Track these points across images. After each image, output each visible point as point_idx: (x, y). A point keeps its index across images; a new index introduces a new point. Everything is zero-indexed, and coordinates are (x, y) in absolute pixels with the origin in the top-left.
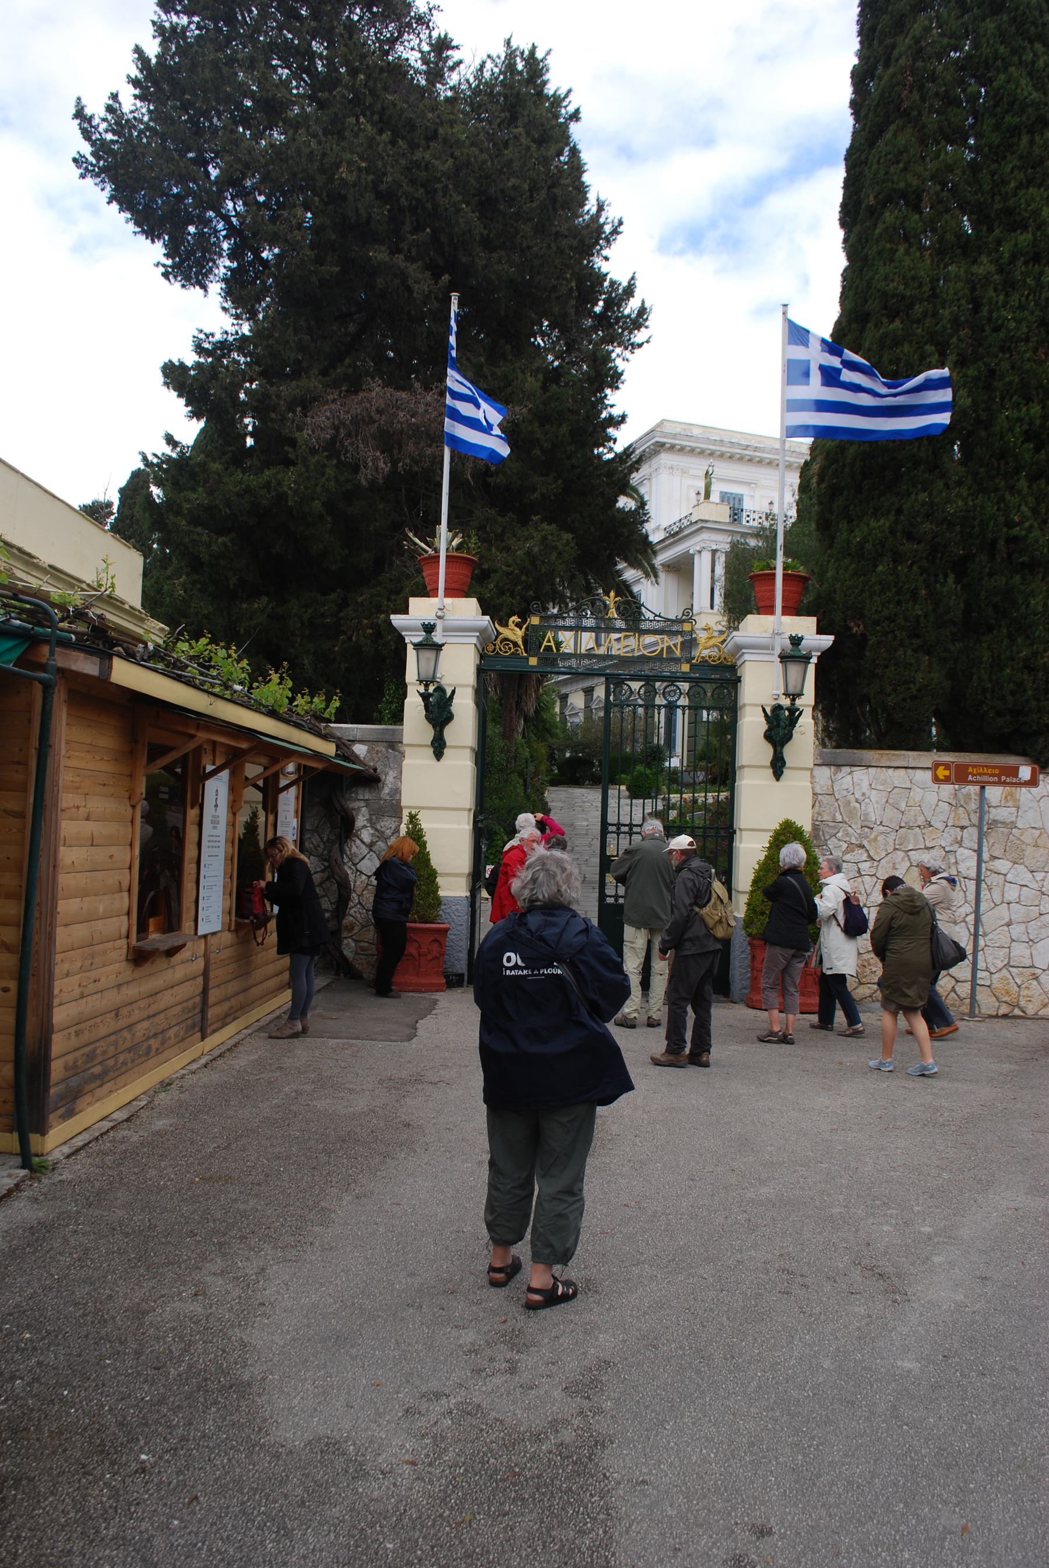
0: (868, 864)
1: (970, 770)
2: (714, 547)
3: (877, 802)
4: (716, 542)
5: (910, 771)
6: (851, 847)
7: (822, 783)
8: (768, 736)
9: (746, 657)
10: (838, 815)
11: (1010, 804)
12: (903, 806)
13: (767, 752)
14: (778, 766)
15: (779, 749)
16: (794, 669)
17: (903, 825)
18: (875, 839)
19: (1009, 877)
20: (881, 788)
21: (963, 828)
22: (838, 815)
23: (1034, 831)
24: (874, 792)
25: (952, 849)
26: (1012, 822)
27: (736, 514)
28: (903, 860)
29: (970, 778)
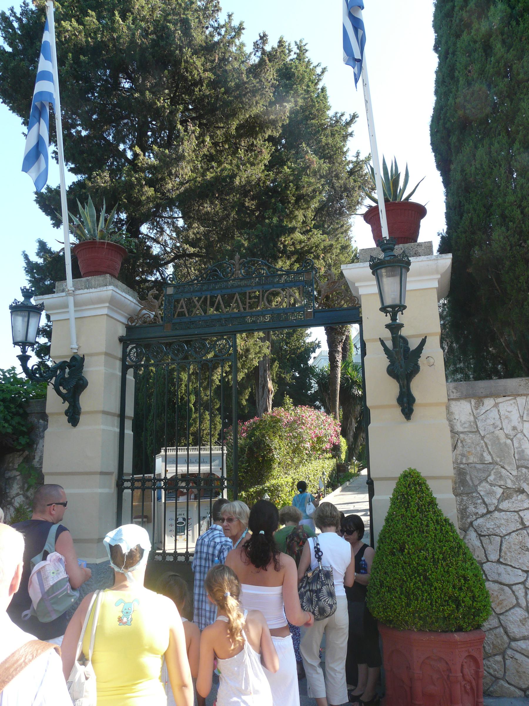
6: (506, 495)
7: (463, 419)
8: (391, 372)
10: (485, 454)
14: (406, 404)
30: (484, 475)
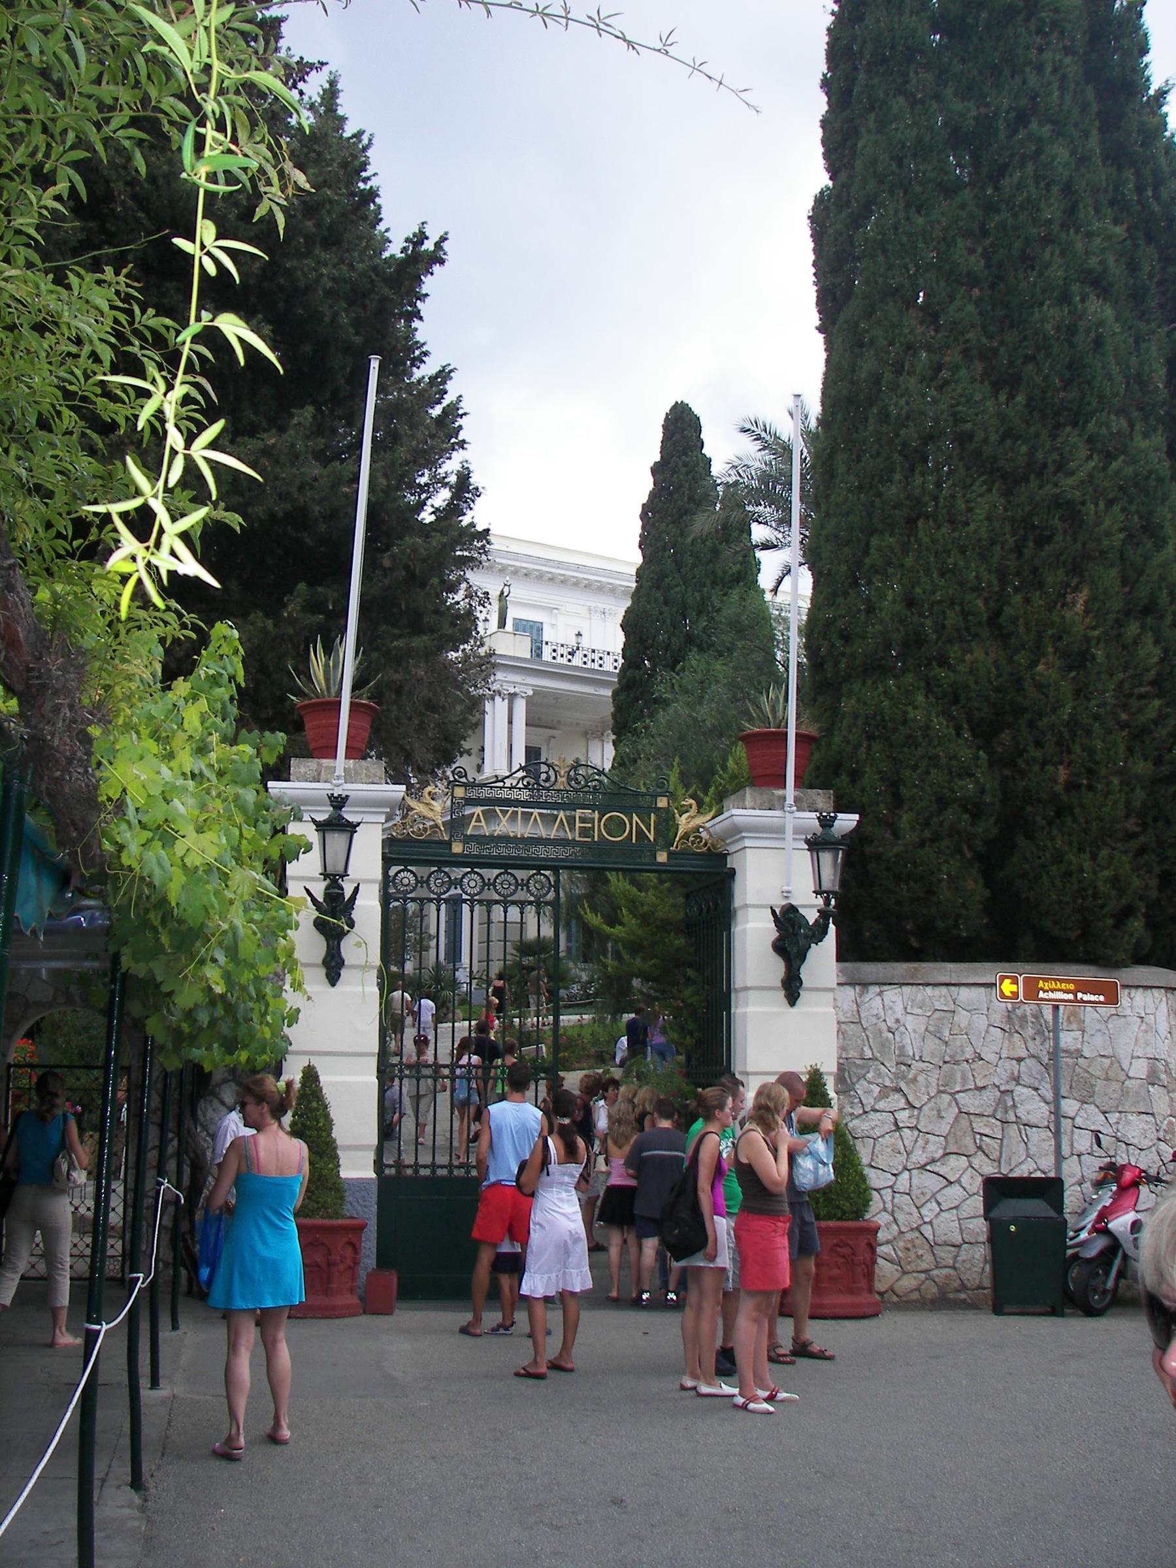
0: (907, 1113)
1: (1041, 984)
2: (512, 690)
3: (915, 1031)
4: (515, 684)
5: (953, 988)
6: (885, 1092)
8: (779, 947)
9: (747, 843)
10: (866, 1049)
11: (1074, 1026)
13: (777, 968)
14: (792, 988)
16: (826, 858)
17: (947, 1059)
18: (914, 1080)
19: (1079, 1121)
20: (919, 1011)
21: (1019, 1060)
22: (866, 1049)
23: (1103, 1060)
24: (909, 1017)
25: (1008, 1087)
26: (1078, 1050)
27: (537, 651)
28: (950, 1105)
29: (1041, 995)
30: (863, 1072)
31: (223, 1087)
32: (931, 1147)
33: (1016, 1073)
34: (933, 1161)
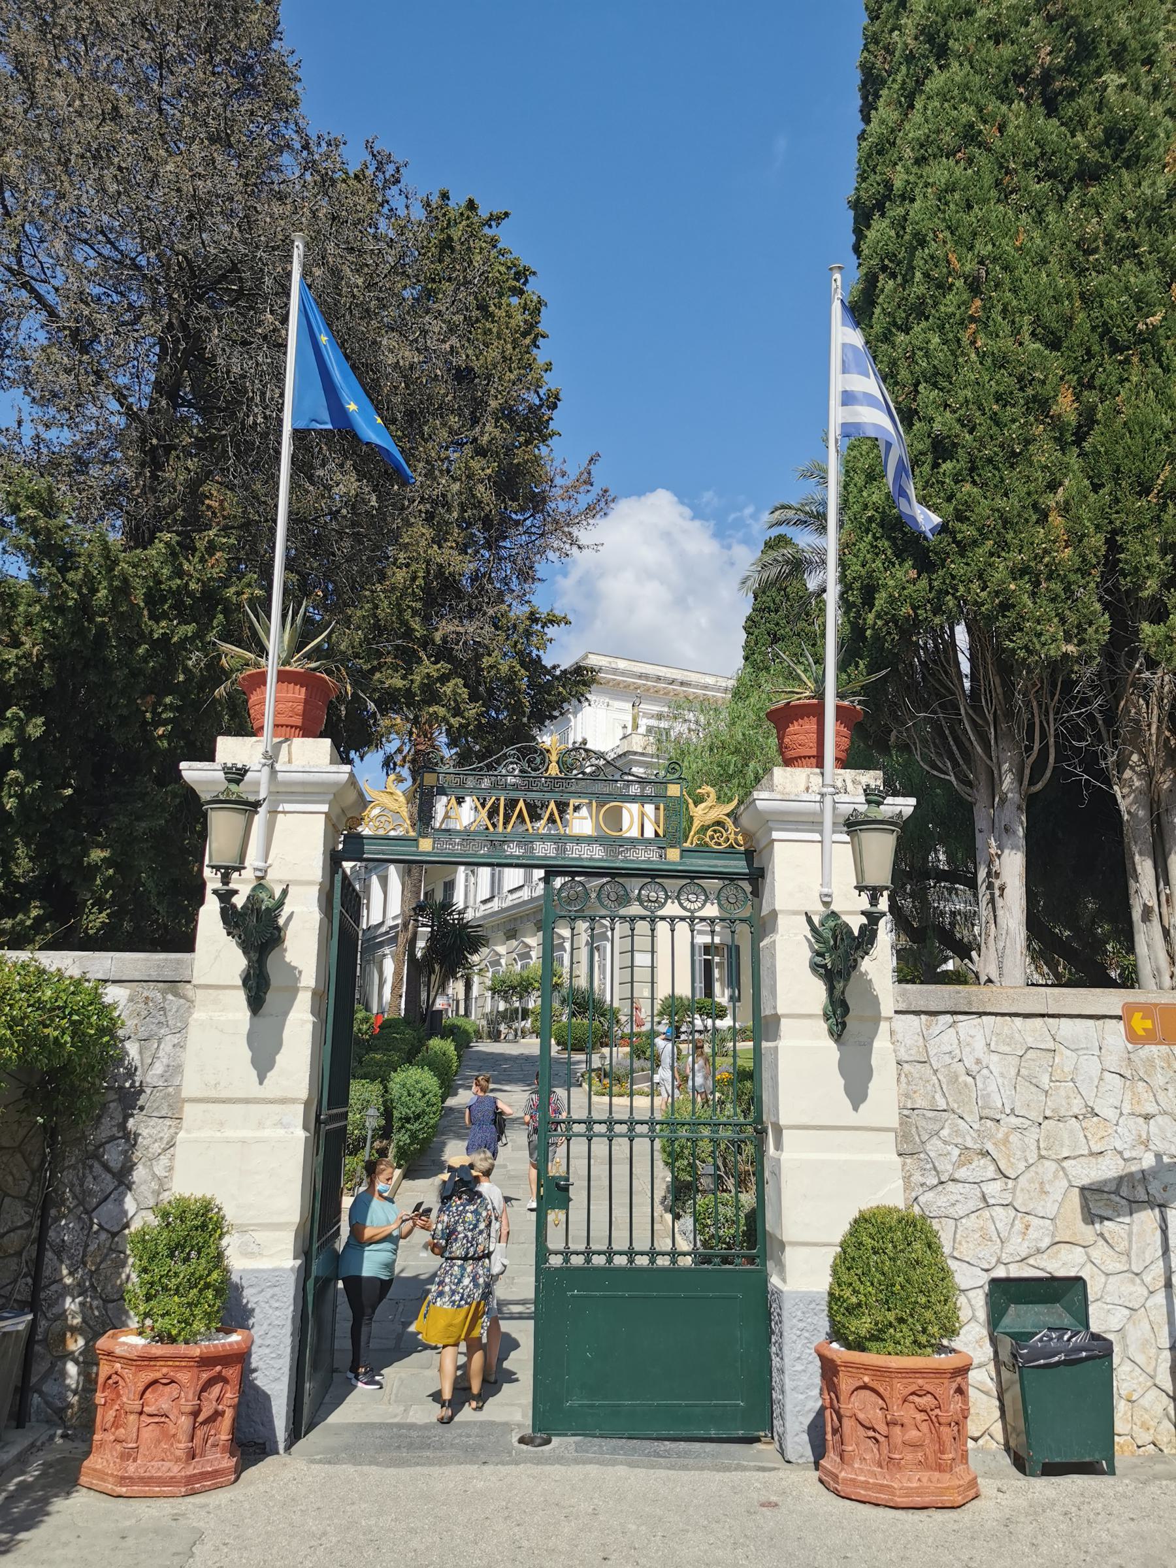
0: (998, 1185)
3: (1002, 1075)
5: (1051, 1020)
7: (909, 1042)
12: (1045, 1081)
13: (816, 993)
15: (839, 986)
17: (1048, 1113)
18: (1006, 1141)
20: (1007, 1049)
21: (1147, 1117)
22: (938, 1096)
24: (995, 1058)
25: (1134, 1154)
28: (1055, 1177)
30: (937, 1128)
31: (108, 1146)
32: (1033, 1234)
33: (1144, 1136)
34: (1039, 1251)
